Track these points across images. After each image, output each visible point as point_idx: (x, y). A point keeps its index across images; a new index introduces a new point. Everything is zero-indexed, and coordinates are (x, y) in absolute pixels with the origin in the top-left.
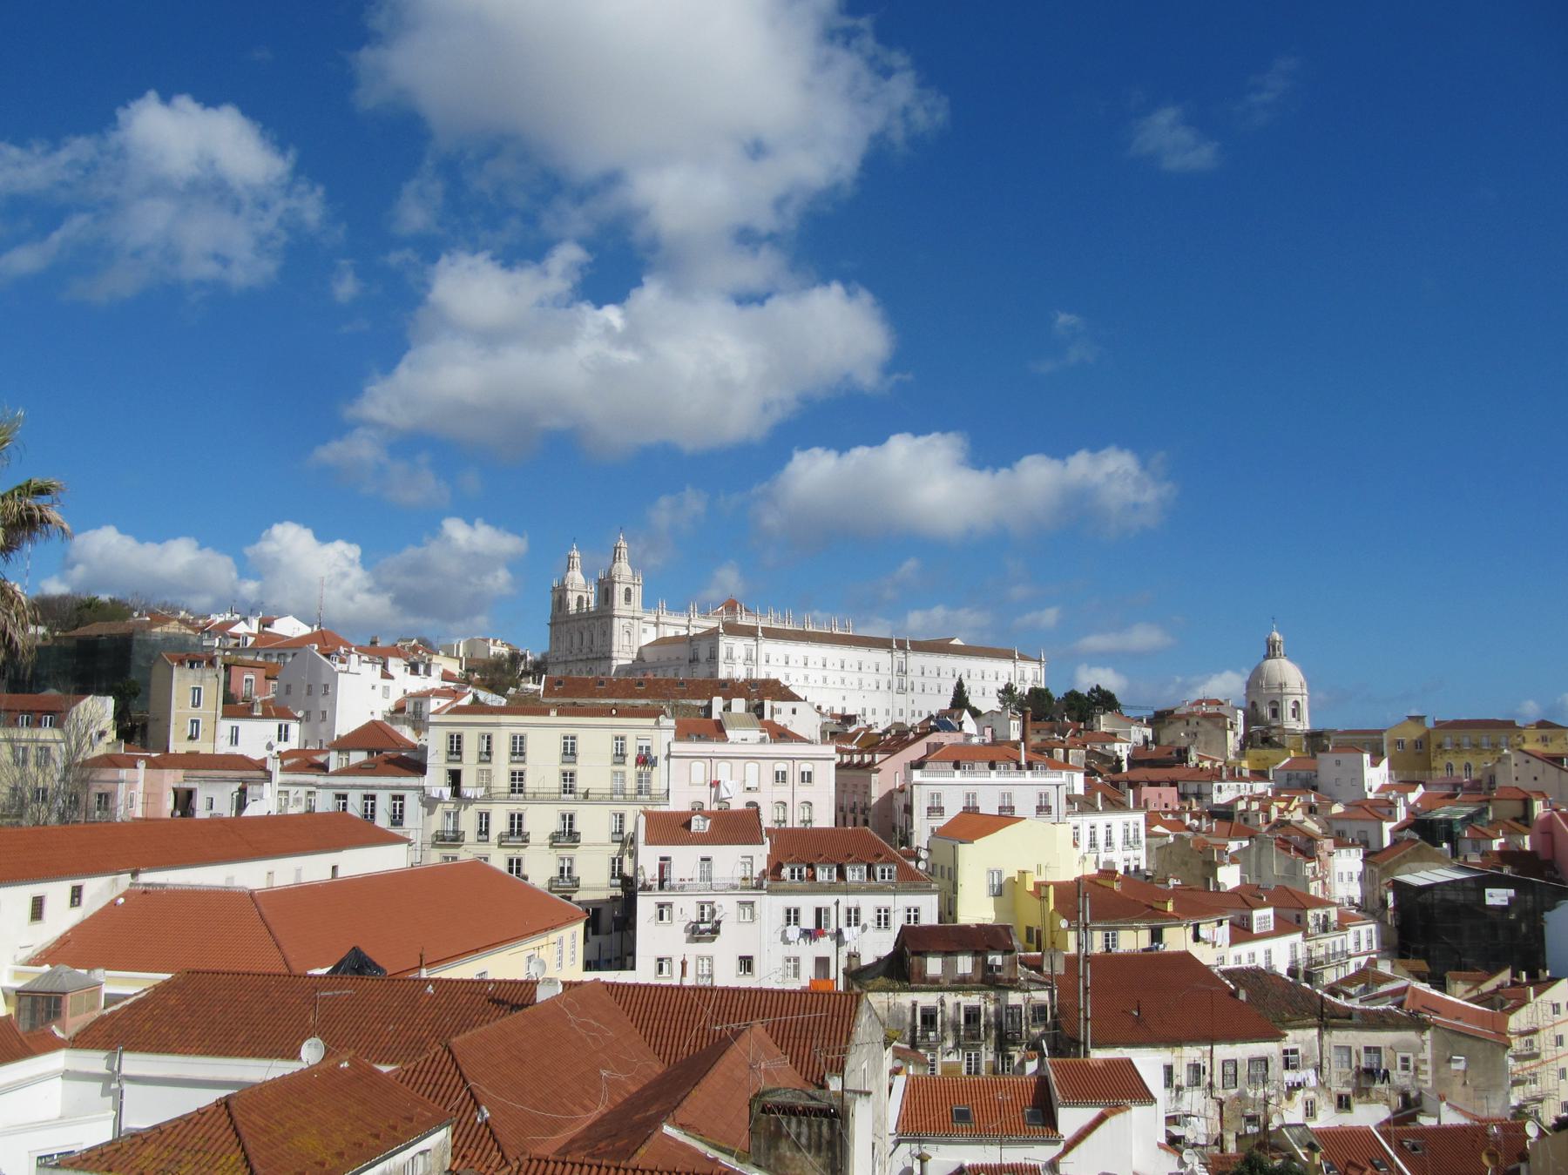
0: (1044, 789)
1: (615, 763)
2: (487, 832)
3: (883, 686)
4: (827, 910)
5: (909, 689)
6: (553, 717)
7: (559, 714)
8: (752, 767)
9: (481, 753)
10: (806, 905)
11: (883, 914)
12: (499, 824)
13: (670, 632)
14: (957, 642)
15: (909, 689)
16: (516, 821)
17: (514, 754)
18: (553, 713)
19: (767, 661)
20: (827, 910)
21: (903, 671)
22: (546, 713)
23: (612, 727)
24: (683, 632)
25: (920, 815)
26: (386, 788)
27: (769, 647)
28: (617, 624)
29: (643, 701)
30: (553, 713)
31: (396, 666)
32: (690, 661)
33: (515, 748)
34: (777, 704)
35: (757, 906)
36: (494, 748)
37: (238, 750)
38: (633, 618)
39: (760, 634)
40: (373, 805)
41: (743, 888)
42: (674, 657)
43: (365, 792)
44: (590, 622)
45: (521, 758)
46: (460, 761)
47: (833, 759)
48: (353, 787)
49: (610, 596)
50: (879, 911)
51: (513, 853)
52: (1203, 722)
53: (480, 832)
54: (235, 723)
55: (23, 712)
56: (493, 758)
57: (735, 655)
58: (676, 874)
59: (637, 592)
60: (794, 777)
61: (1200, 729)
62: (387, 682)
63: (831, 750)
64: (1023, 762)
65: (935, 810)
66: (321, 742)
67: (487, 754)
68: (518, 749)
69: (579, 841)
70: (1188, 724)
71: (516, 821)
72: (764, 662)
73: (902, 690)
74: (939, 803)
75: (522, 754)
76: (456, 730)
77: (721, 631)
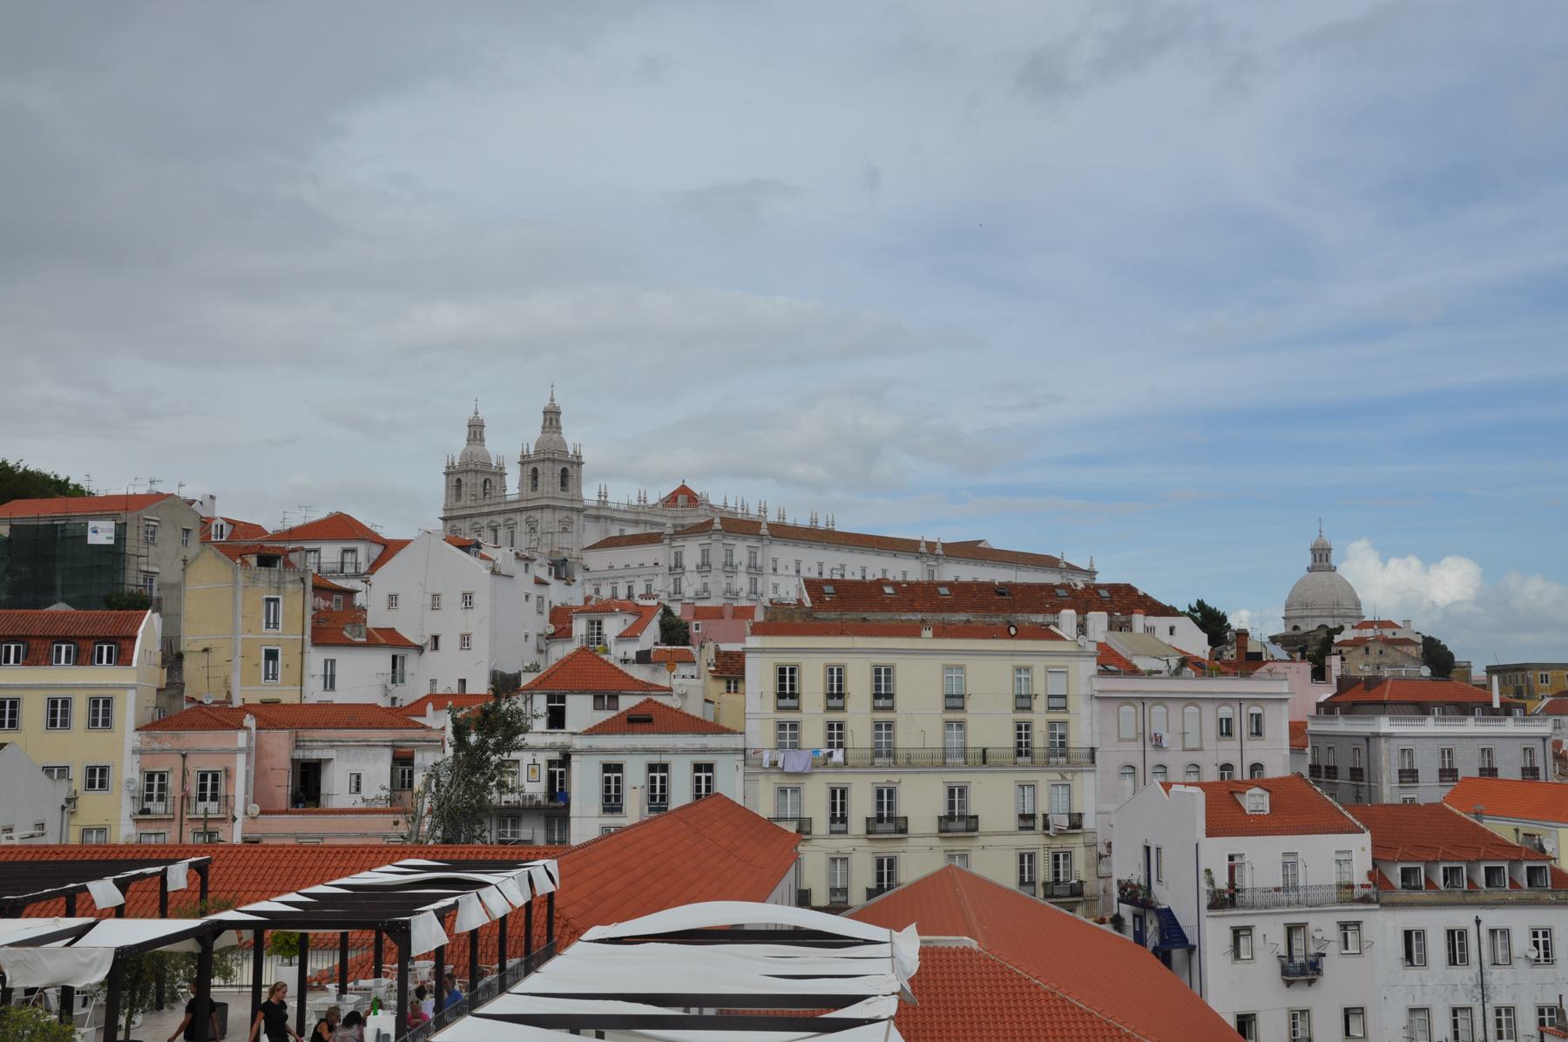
0: (1528, 744)
2: (844, 819)
4: (1462, 934)
6: (927, 640)
7: (936, 635)
8: (1192, 709)
9: (830, 696)
10: (1435, 923)
11: (1541, 939)
12: (861, 807)
13: (615, 531)
16: (885, 796)
17: (877, 696)
20: (1462, 934)
22: (913, 631)
23: (1013, 653)
24: (630, 531)
25: (1390, 782)
26: (686, 751)
29: (961, 617)
30: (928, 633)
31: (541, 565)
32: (670, 569)
33: (878, 687)
34: (1152, 621)
35: (1364, 927)
37: (339, 697)
38: (572, 509)
39: (764, 531)
40: (708, 779)
41: (1342, 902)
42: (634, 564)
43: (655, 759)
44: (507, 516)
45: (888, 703)
46: (797, 709)
48: (633, 751)
50: (1535, 935)
51: (886, 849)
52: (1388, 650)
53: (833, 819)
54: (330, 654)
55: (105, 640)
56: (851, 704)
57: (736, 561)
58: (1247, 881)
60: (1242, 726)
61: (1383, 660)
62: (541, 590)
64: (1496, 704)
65: (1409, 775)
66: (463, 682)
67: (836, 694)
68: (883, 694)
69: (976, 829)
70: (1367, 650)
71: (885, 796)
72: (771, 571)
74: (1411, 763)
75: (889, 696)
76: (787, 660)
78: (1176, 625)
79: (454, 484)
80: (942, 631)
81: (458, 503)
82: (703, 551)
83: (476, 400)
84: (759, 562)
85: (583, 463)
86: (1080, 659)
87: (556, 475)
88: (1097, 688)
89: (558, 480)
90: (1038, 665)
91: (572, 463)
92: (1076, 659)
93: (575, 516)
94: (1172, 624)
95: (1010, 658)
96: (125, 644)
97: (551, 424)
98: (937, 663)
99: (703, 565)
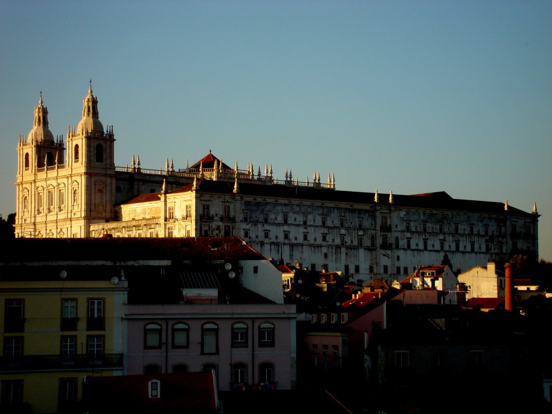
3: (367, 242)
5: (394, 246)
15: (394, 246)
21: (386, 228)
23: (62, 290)
47: (295, 318)
57: (212, 212)
63: (293, 308)
73: (386, 246)
78: (258, 266)
79: (24, 157)
81: (27, 172)
82: (187, 207)
83: (41, 93)
84: (232, 214)
85: (115, 140)
86: (115, 292)
87: (92, 149)
88: (127, 313)
91: (105, 140)
92: (111, 293)
94: (256, 265)
95: (60, 293)
97: (89, 111)
99: (187, 216)
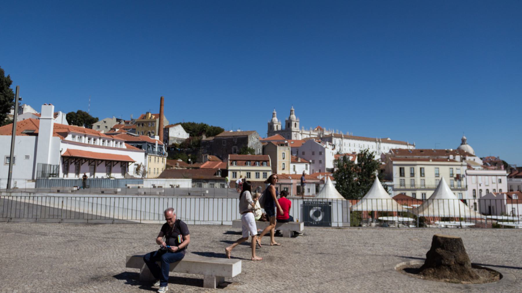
1: (436, 177)
6: (431, 162)
9: (411, 174)
14: (389, 139)
18: (431, 161)
19: (345, 145)
22: (428, 160)
24: (308, 136)
27: (345, 141)
28: (293, 134)
30: (431, 161)
36: (415, 172)
38: (297, 132)
44: (283, 133)
49: (290, 125)
56: (415, 175)
59: (298, 124)
77: (333, 136)
80: (434, 160)
89: (294, 125)
90: (454, 167)
93: (298, 133)
96: (268, 162)
98: (433, 167)
